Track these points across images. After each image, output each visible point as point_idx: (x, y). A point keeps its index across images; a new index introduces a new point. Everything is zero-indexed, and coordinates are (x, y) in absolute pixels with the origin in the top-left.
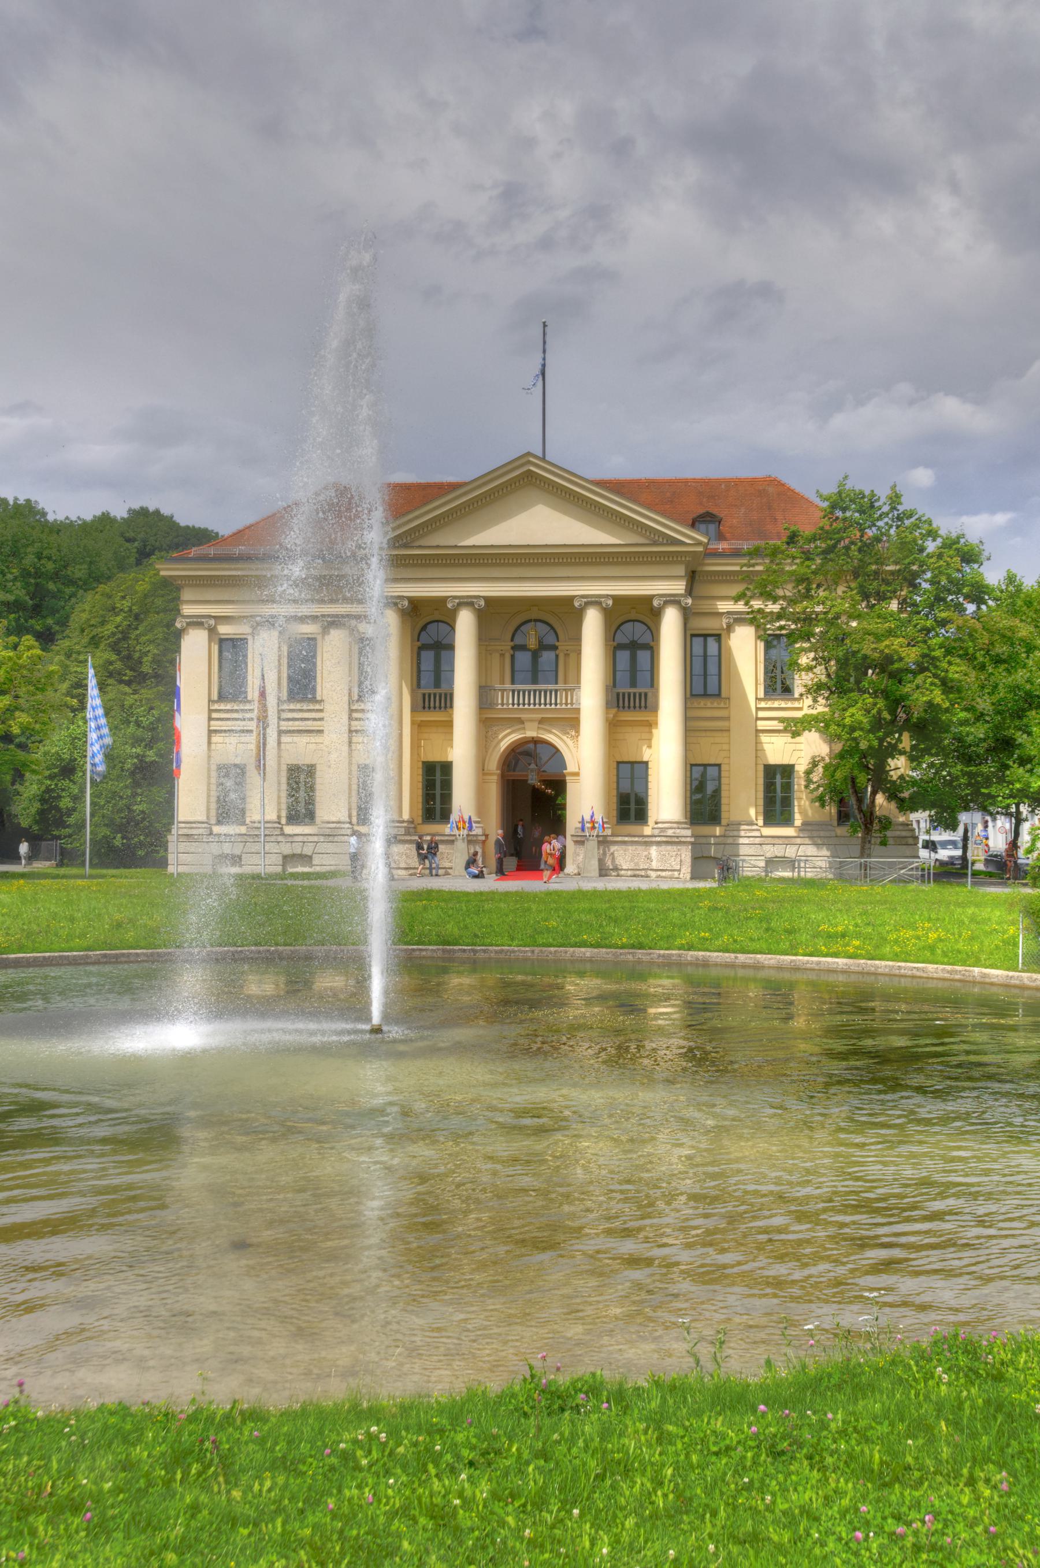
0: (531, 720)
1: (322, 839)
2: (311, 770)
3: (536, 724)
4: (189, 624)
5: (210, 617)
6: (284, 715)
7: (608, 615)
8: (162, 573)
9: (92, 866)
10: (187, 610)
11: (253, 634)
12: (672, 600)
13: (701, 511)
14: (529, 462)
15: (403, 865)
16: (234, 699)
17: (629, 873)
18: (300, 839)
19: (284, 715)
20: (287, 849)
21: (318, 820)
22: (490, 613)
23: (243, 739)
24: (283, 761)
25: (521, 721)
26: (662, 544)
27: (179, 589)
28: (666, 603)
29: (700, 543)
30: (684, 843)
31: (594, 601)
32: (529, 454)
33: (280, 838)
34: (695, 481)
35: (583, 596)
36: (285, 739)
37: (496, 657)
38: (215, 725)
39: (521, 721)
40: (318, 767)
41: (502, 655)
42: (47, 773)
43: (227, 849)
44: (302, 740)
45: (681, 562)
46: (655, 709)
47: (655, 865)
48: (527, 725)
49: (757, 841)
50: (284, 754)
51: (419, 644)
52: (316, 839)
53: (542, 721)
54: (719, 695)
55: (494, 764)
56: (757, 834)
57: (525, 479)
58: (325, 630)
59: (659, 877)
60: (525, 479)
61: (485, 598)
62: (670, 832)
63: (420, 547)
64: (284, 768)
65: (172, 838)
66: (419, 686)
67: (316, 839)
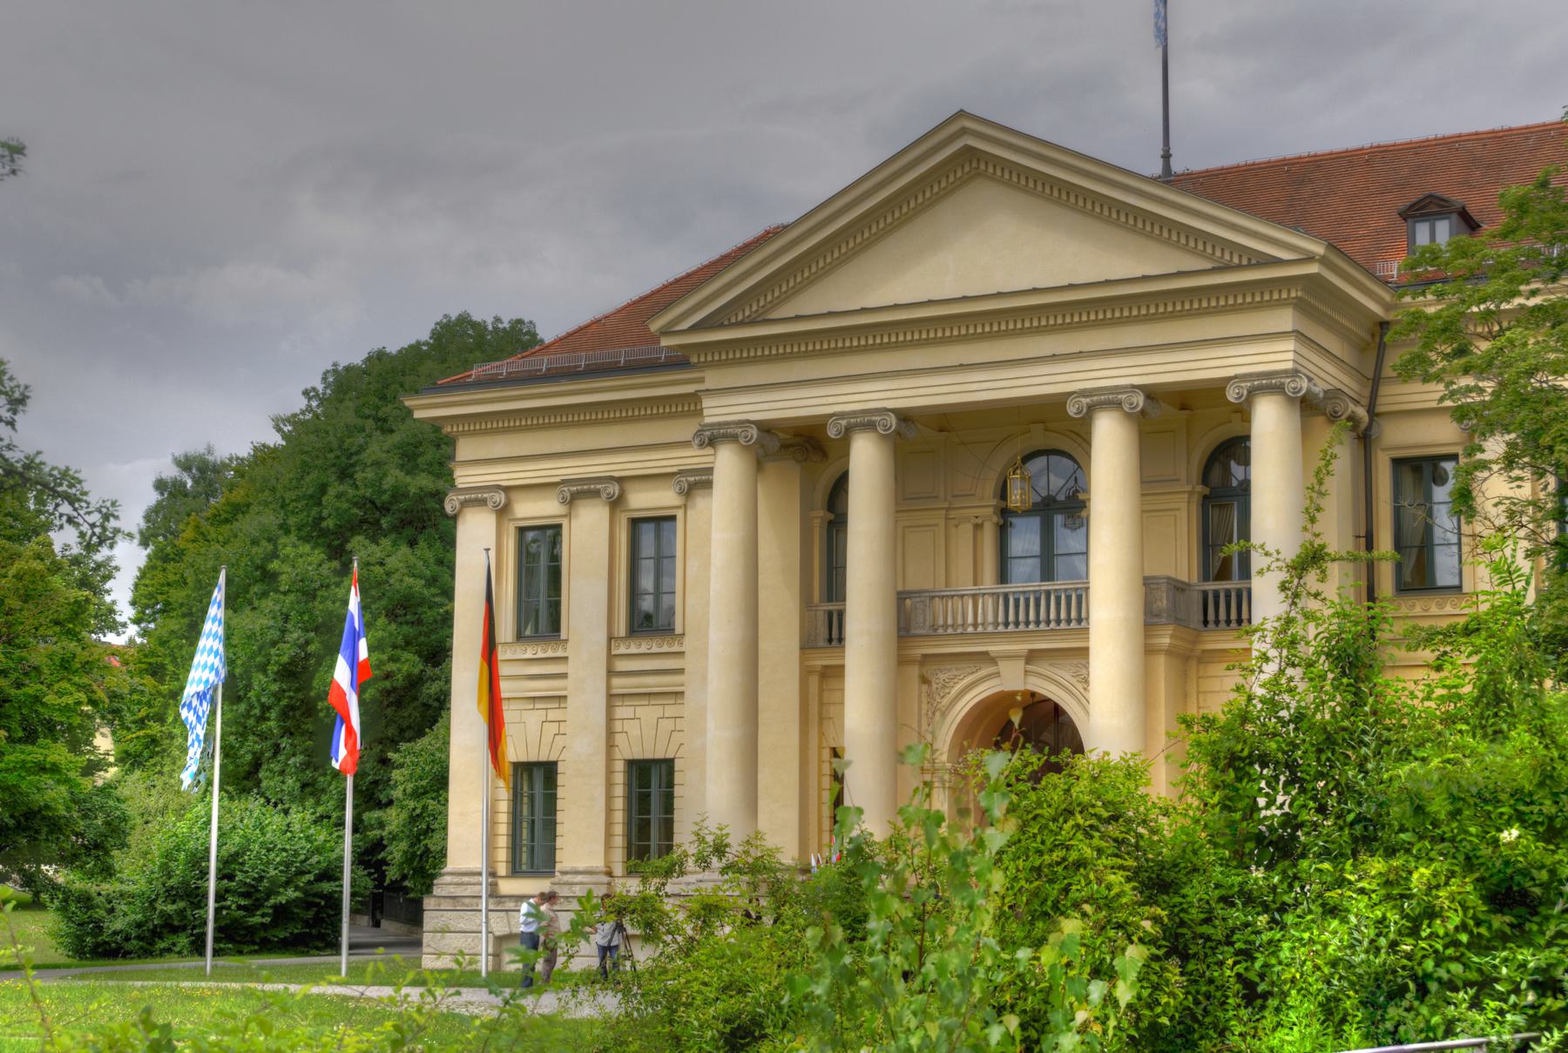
2: (667, 766)
3: (1021, 664)
4: (465, 504)
5: (499, 487)
6: (621, 666)
8: (418, 414)
9: (217, 953)
10: (465, 477)
11: (569, 515)
12: (1269, 384)
13: (1414, 196)
14: (964, 131)
19: (621, 666)
22: (924, 442)
23: (552, 715)
24: (618, 755)
25: (985, 658)
26: (1239, 267)
27: (451, 442)
28: (1253, 393)
29: (1310, 258)
31: (1108, 400)
32: (961, 114)
34: (1476, 137)
35: (1084, 393)
36: (622, 712)
37: (967, 529)
40: (678, 765)
41: (978, 527)
42: (410, 787)
44: (648, 712)
45: (1280, 304)
48: (1003, 666)
50: (620, 739)
53: (1032, 657)
54: (1459, 588)
57: (959, 162)
60: (959, 162)
61: (893, 411)
63: (798, 318)
64: (620, 766)
65: (428, 903)
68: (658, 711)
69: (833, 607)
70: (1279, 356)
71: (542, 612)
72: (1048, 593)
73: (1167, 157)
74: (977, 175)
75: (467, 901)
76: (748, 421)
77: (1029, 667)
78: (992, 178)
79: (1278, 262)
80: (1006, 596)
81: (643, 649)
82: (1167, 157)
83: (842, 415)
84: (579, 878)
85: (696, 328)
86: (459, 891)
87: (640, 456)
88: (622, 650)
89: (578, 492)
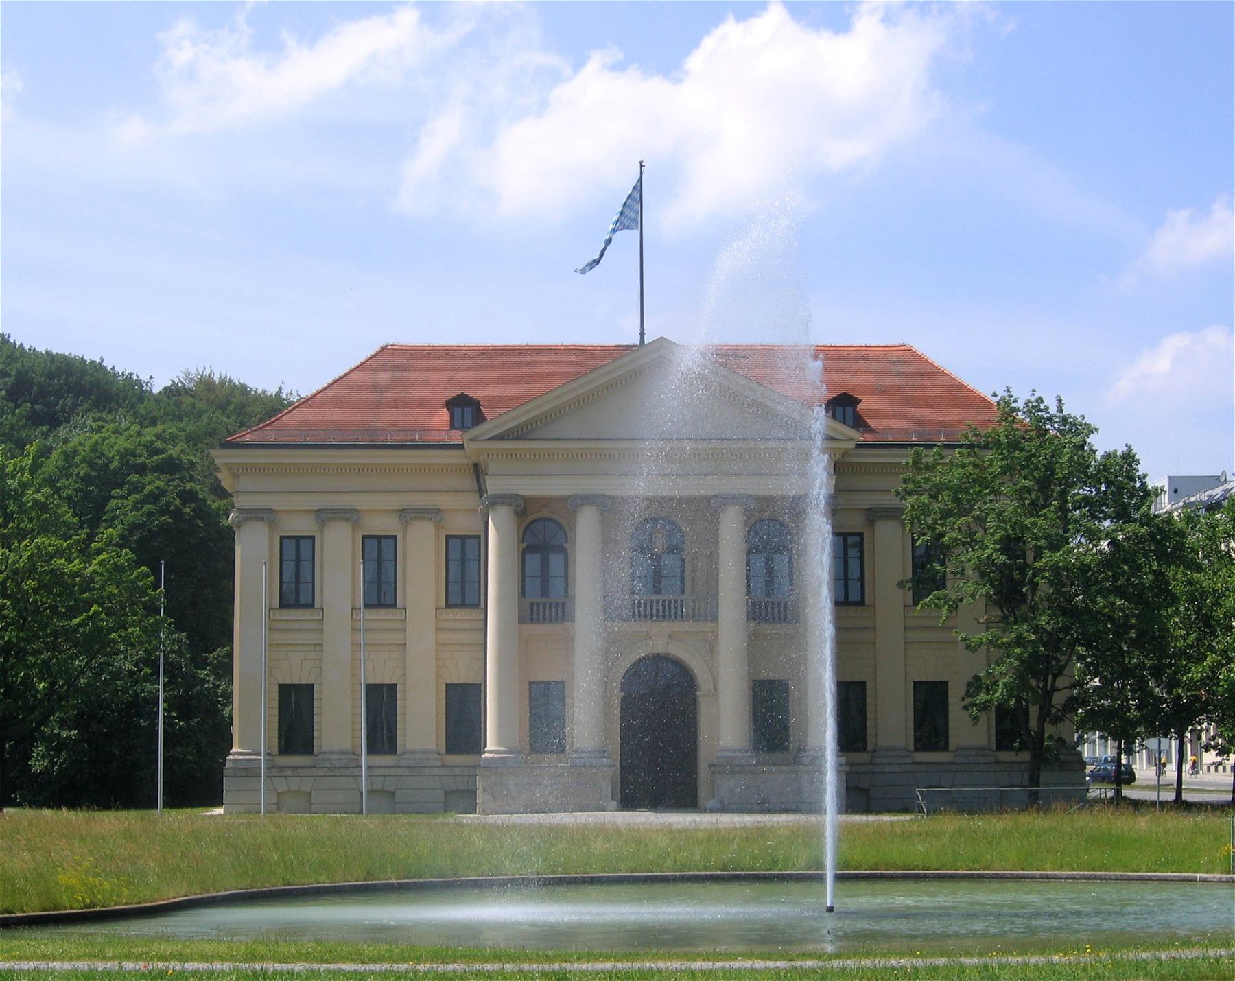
1: (405, 771)
7: (748, 513)
10: (241, 501)
16: (298, 605)
18: (382, 771)
29: (851, 440)
46: (797, 621)
49: (910, 768)
51: (525, 545)
52: (399, 771)
54: (861, 603)
55: (616, 685)
56: (909, 760)
58: (406, 524)
66: (523, 593)
71: (296, 592)
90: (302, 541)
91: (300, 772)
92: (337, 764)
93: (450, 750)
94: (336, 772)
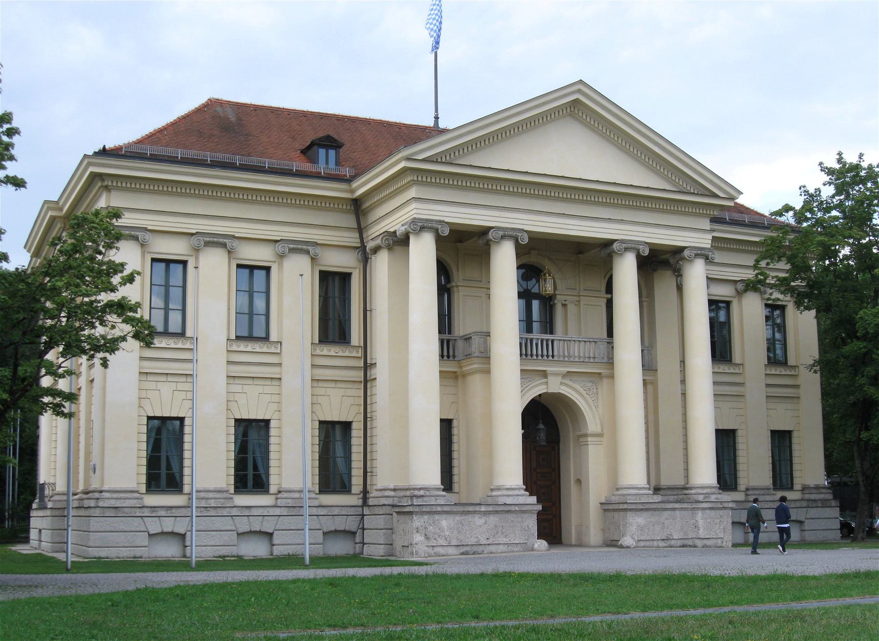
0: (556, 374)
1: (285, 512)
14: (579, 91)
15: (454, 542)
17: (679, 543)
18: (260, 512)
20: (244, 525)
21: (273, 489)
23: (181, 386)
25: (544, 374)
28: (697, 255)
30: (725, 508)
33: (234, 512)
35: (622, 241)
38: (149, 366)
39: (544, 374)
43: (169, 525)
47: (702, 533)
48: (550, 379)
52: (278, 511)
59: (704, 546)
62: (713, 498)
67: (278, 511)
68: (260, 389)
69: (446, 337)
70: (704, 241)
72: (547, 340)
73: (437, 118)
74: (572, 115)
75: (126, 510)
76: (443, 221)
77: (563, 381)
78: (576, 119)
79: (715, 196)
80: (531, 340)
81: (249, 349)
82: (437, 118)
83: (499, 228)
84: (211, 495)
85: (424, 160)
86: (118, 504)
87: (257, 228)
88: (234, 348)
89: (209, 242)
90: (172, 266)
91: (175, 512)
92: (213, 503)
93: (321, 492)
94: (212, 512)
